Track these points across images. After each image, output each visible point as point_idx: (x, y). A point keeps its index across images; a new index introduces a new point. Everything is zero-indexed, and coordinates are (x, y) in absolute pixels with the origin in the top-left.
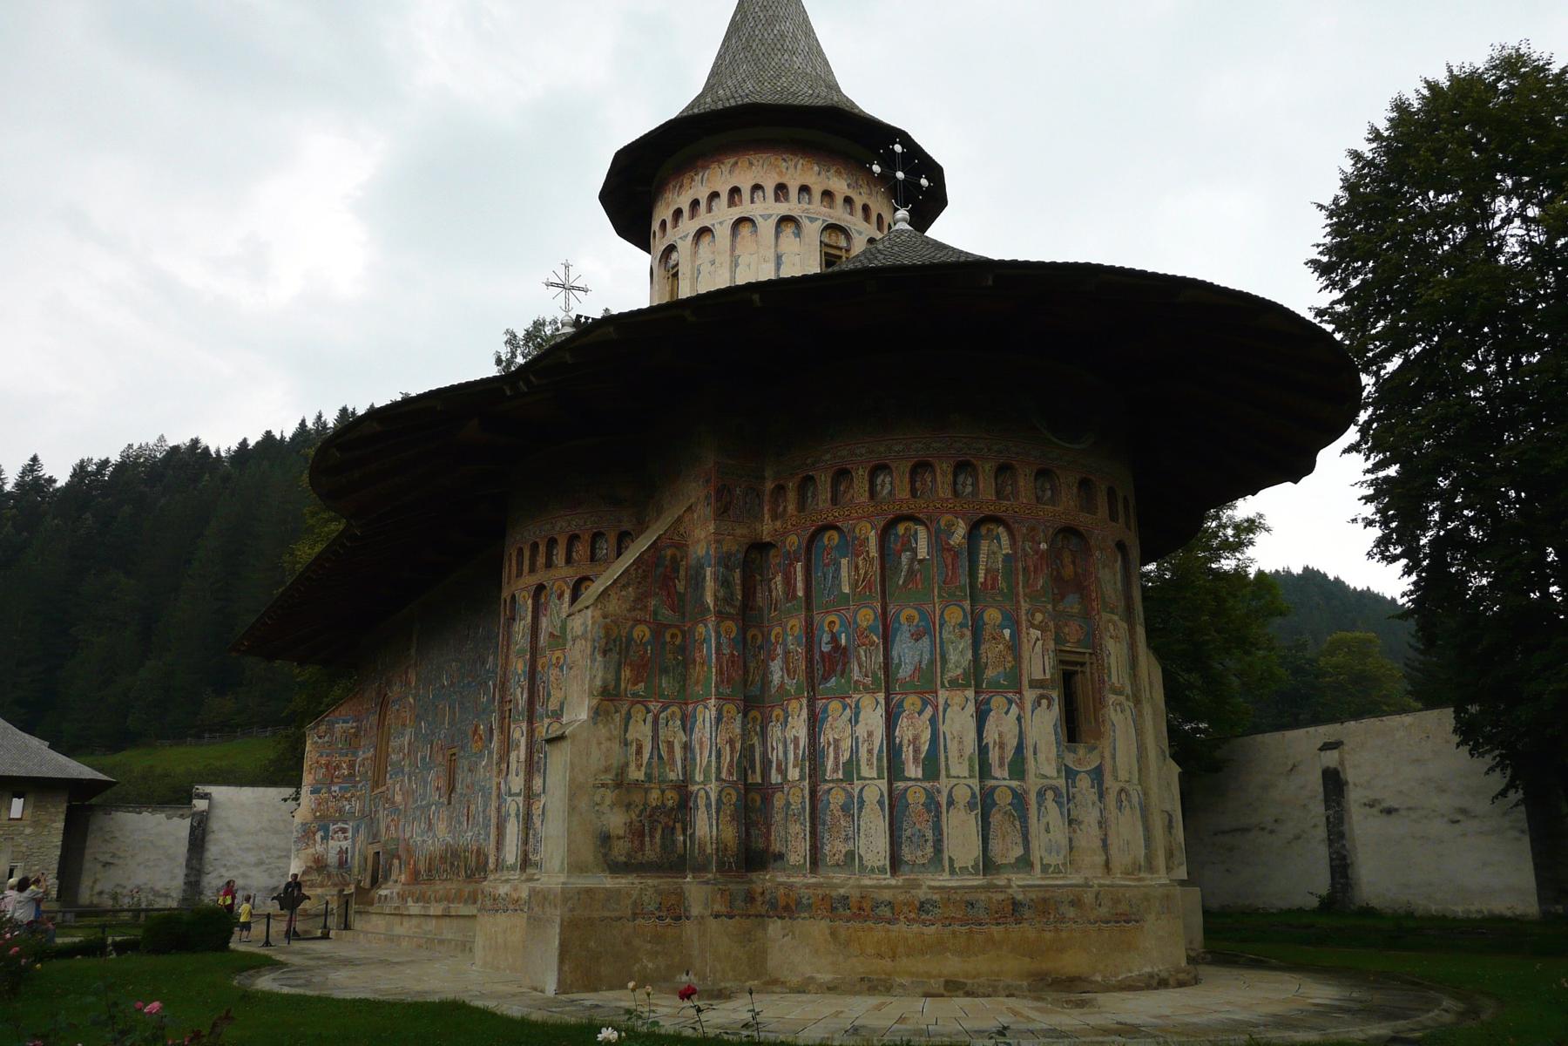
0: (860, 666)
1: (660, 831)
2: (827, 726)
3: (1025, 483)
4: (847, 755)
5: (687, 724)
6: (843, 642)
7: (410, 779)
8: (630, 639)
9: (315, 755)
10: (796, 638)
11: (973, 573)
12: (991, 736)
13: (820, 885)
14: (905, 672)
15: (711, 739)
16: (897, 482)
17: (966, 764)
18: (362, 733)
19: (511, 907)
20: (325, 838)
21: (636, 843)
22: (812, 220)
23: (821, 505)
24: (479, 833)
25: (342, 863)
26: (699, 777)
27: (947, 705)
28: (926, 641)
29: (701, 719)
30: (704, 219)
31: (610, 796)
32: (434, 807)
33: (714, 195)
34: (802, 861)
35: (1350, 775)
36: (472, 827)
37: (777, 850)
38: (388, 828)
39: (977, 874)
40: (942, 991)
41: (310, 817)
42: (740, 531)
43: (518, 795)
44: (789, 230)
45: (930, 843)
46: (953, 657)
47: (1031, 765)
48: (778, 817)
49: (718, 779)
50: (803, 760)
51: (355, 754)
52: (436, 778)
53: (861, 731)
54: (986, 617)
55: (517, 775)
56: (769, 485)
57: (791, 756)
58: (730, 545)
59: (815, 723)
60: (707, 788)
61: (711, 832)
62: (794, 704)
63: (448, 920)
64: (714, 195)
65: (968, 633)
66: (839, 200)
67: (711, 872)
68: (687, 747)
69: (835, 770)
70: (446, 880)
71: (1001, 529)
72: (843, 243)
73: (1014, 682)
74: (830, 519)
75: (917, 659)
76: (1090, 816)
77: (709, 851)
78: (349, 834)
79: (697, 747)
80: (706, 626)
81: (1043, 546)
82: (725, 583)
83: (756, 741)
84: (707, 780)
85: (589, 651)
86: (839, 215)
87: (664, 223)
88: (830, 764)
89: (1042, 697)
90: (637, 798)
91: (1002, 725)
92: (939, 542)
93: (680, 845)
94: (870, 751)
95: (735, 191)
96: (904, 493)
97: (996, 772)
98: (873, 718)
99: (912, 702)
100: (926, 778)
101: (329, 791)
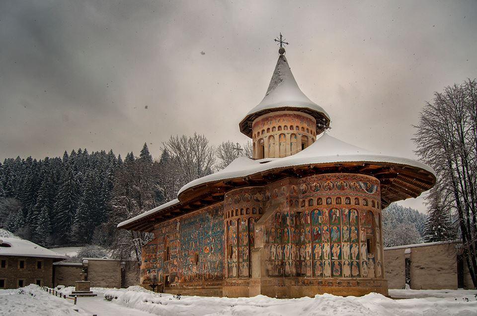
5: (283, 248)
10: (309, 232)
13: (315, 279)
14: (334, 239)
20: (149, 272)
27: (344, 246)
30: (271, 133)
35: (413, 260)
44: (294, 136)
46: (345, 236)
53: (324, 250)
57: (307, 255)
59: (313, 249)
62: (308, 245)
68: (283, 253)
69: (318, 258)
79: (286, 253)
87: (259, 133)
88: (316, 257)
95: (280, 127)
98: (327, 248)
99: (336, 245)
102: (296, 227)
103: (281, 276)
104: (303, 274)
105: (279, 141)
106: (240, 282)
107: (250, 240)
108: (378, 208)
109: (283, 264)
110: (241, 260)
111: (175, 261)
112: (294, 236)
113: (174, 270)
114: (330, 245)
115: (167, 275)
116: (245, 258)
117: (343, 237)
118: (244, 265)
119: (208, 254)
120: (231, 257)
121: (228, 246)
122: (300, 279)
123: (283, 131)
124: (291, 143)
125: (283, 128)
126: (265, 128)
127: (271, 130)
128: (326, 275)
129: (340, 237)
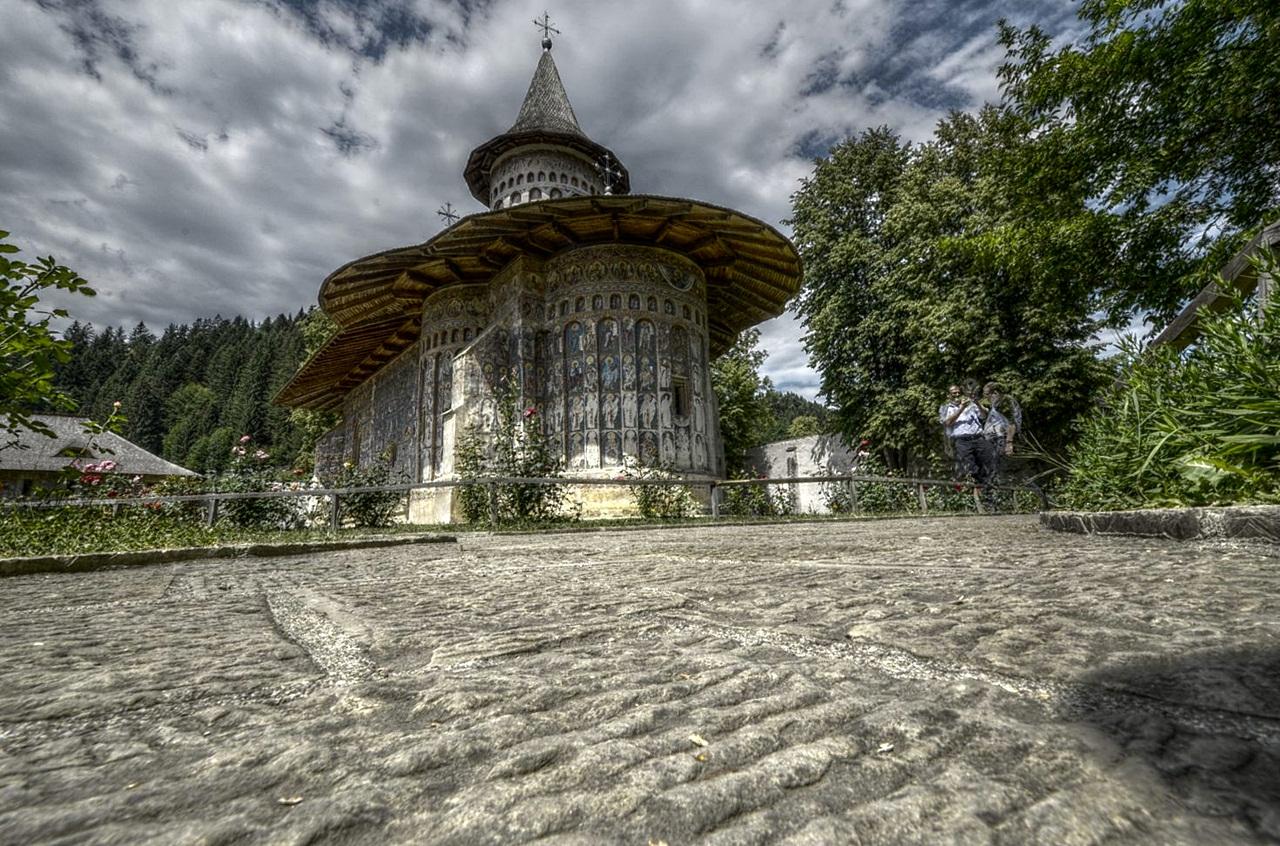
11: (637, 343)
12: (644, 412)
14: (607, 384)
33: (521, 176)
42: (535, 324)
46: (628, 377)
47: (660, 424)
51: (342, 451)
53: (588, 408)
56: (549, 305)
59: (568, 406)
64: (521, 176)
66: (580, 183)
73: (654, 387)
76: (685, 446)
82: (527, 346)
87: (496, 191)
88: (574, 424)
91: (649, 408)
92: (623, 329)
95: (531, 175)
96: (607, 307)
98: (593, 404)
100: (616, 428)
108: (698, 322)
117: (624, 379)
119: (409, 441)
123: (535, 183)
125: (536, 176)
126: (506, 179)
127: (515, 182)
128: (590, 464)
129: (619, 380)
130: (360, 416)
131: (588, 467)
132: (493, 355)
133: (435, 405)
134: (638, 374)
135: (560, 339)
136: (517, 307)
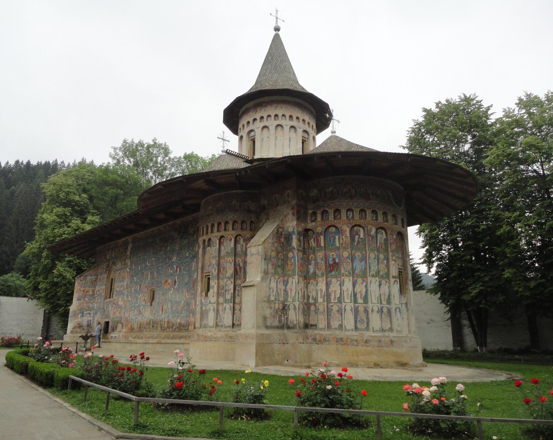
0: (344, 268)
1: (278, 318)
2: (331, 286)
3: (390, 218)
4: (338, 296)
5: (286, 283)
6: (337, 261)
7: (127, 296)
8: (271, 256)
9: (79, 287)
10: (322, 259)
11: (377, 244)
14: (357, 271)
15: (296, 288)
16: (355, 214)
17: (377, 300)
18: (98, 280)
19: (213, 339)
20: (82, 316)
21: (273, 320)
22: (300, 128)
23: (330, 219)
24: (169, 316)
25: (89, 325)
26: (290, 300)
27: (371, 282)
28: (363, 262)
29: (291, 282)
31: (266, 305)
32: (142, 307)
34: (324, 327)
36: (165, 314)
37: (312, 324)
38: (114, 313)
39: (380, 332)
40: (373, 367)
41: (76, 309)
42: (303, 225)
43: (214, 303)
44: (293, 130)
45: (365, 323)
46: (372, 268)
48: (312, 313)
49: (298, 301)
50: (324, 296)
51: (95, 287)
52: (143, 297)
53: (344, 288)
54: (380, 257)
55: (213, 297)
56: (310, 212)
57: (319, 295)
58: (300, 229)
59: (328, 285)
60: (294, 303)
61: (296, 317)
63: (159, 345)
64: (269, 116)
65: (376, 261)
67: (297, 329)
68: (285, 291)
70: (150, 331)
71: (383, 231)
72: (307, 136)
73: (387, 275)
74: (333, 223)
75: (361, 267)
76: (406, 317)
77: (295, 323)
78: (92, 315)
80: (293, 253)
81: (395, 237)
82: (299, 240)
83: (305, 289)
84: (294, 300)
85: (260, 258)
86: (306, 127)
87: (248, 123)
88: (332, 298)
89: (395, 281)
90: (273, 305)
92: (367, 233)
93: (283, 321)
94: (348, 294)
95: (276, 116)
97: (383, 302)
98: (348, 284)
99: (360, 280)
101: (84, 300)
102: (304, 251)
103: (281, 327)
104: (312, 325)
105: (276, 134)
106: (219, 334)
107: (235, 270)
109: (285, 308)
110: (221, 300)
111: (120, 299)
112: (301, 265)
113: (117, 313)
114: (353, 280)
115: (107, 320)
116: (229, 296)
117: (370, 269)
118: (225, 309)
120: (206, 295)
121: (202, 278)
122: (310, 332)
124: (290, 139)
126: (258, 116)
128: (348, 327)
129: (366, 269)
130: (114, 263)
131: (346, 330)
132: (276, 245)
133: (218, 273)
134: (378, 264)
135: (322, 237)
136: (291, 212)
